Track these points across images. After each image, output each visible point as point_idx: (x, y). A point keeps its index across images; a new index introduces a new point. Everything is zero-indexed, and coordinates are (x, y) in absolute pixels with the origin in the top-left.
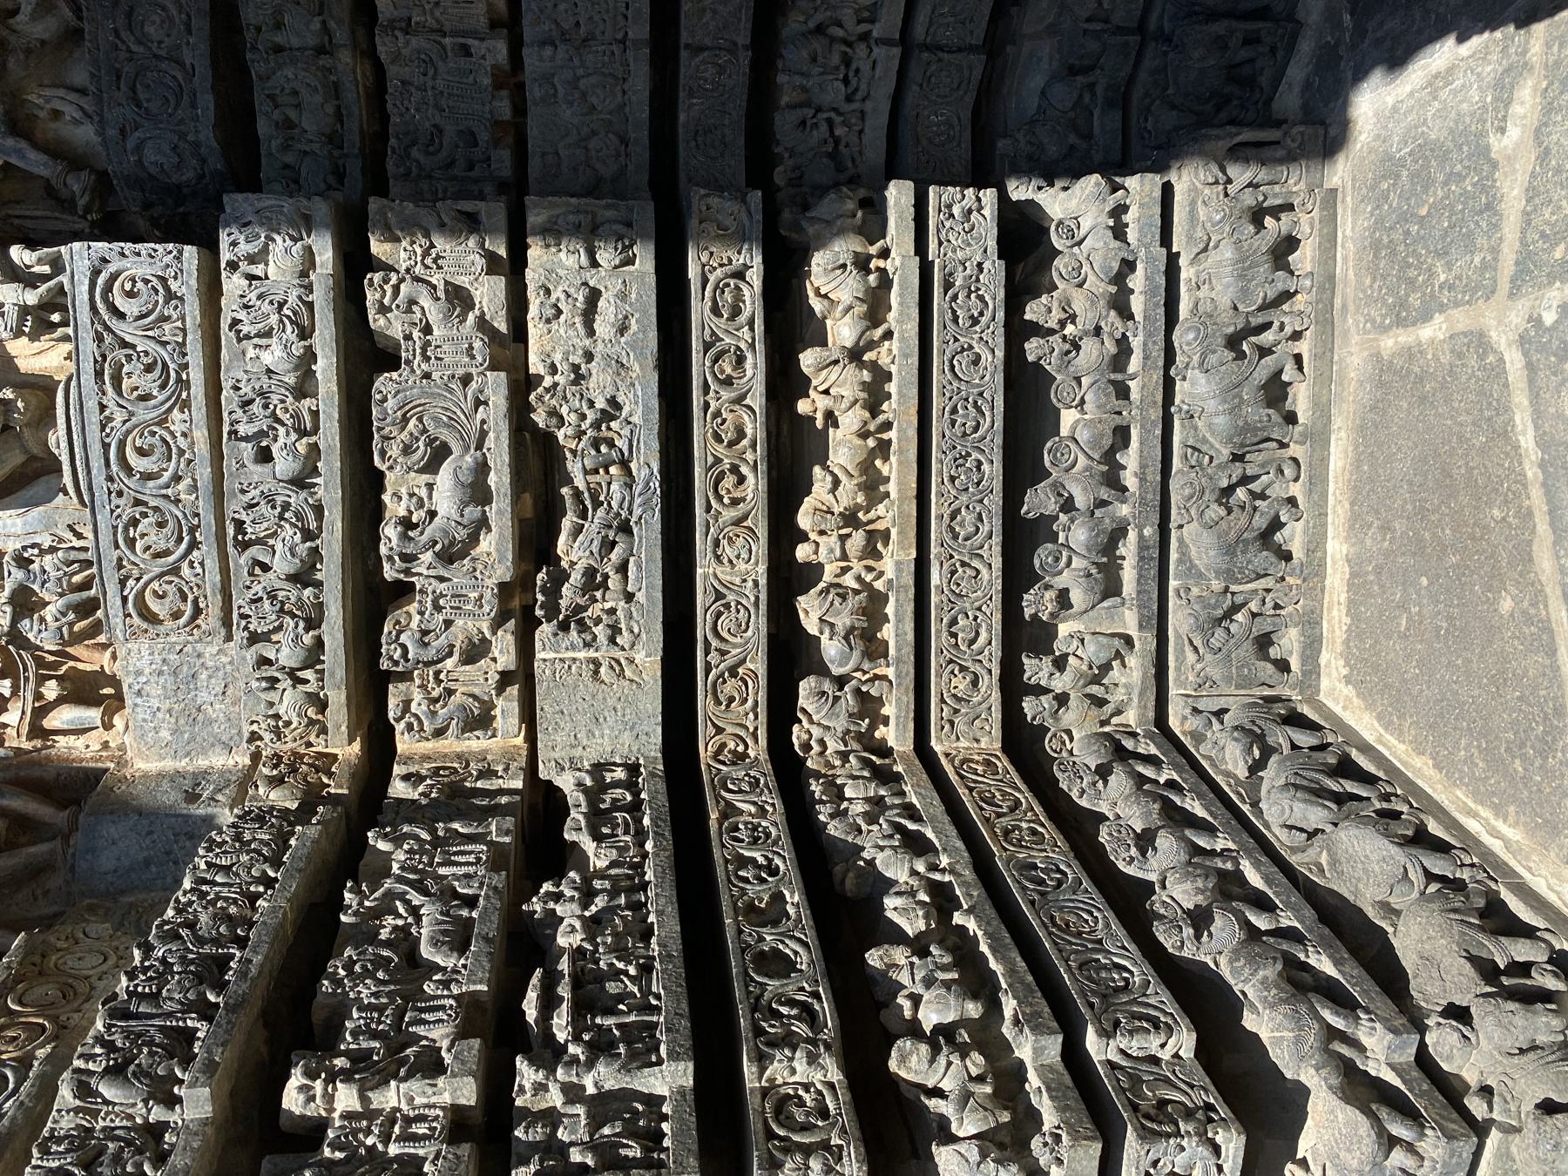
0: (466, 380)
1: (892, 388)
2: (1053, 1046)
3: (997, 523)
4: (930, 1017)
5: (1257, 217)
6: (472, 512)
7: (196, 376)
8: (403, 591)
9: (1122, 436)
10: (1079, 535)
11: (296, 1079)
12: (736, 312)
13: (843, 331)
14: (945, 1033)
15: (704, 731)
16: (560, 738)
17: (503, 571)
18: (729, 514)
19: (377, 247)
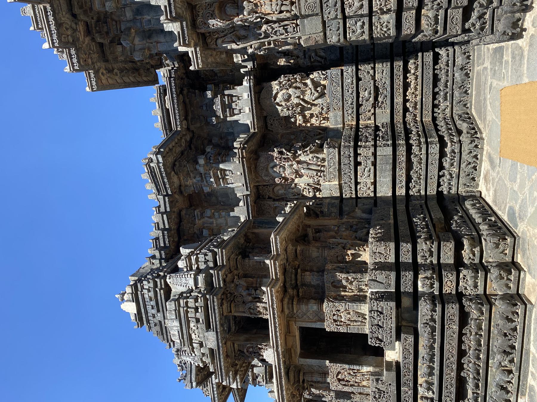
0: (369, 81)
1: (419, 77)
2: (424, 140)
3: (432, 93)
4: (414, 139)
5: (465, 53)
6: (369, 96)
7: (340, 83)
8: (362, 105)
9: (447, 81)
10: (442, 93)
11: (359, 142)
12: (399, 70)
13: (412, 71)
14: (415, 140)
15: (395, 119)
16: (379, 120)
17: (373, 102)
18: (398, 94)
19: (359, 67)
